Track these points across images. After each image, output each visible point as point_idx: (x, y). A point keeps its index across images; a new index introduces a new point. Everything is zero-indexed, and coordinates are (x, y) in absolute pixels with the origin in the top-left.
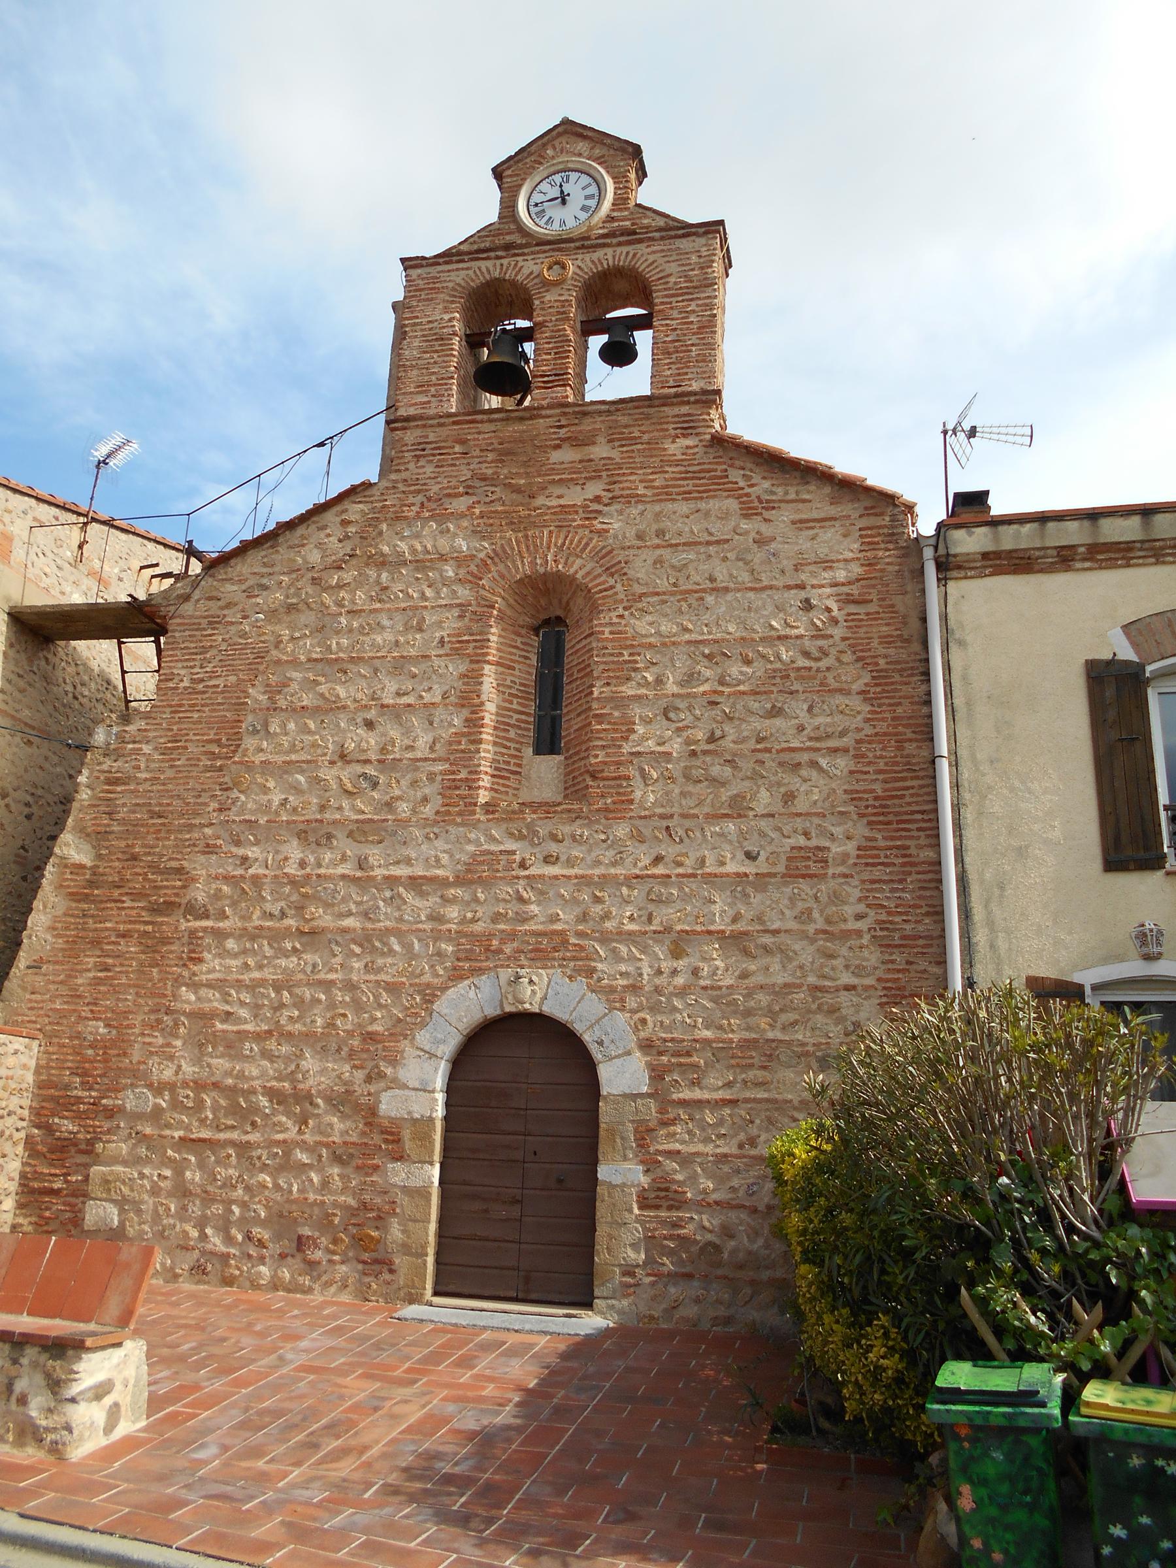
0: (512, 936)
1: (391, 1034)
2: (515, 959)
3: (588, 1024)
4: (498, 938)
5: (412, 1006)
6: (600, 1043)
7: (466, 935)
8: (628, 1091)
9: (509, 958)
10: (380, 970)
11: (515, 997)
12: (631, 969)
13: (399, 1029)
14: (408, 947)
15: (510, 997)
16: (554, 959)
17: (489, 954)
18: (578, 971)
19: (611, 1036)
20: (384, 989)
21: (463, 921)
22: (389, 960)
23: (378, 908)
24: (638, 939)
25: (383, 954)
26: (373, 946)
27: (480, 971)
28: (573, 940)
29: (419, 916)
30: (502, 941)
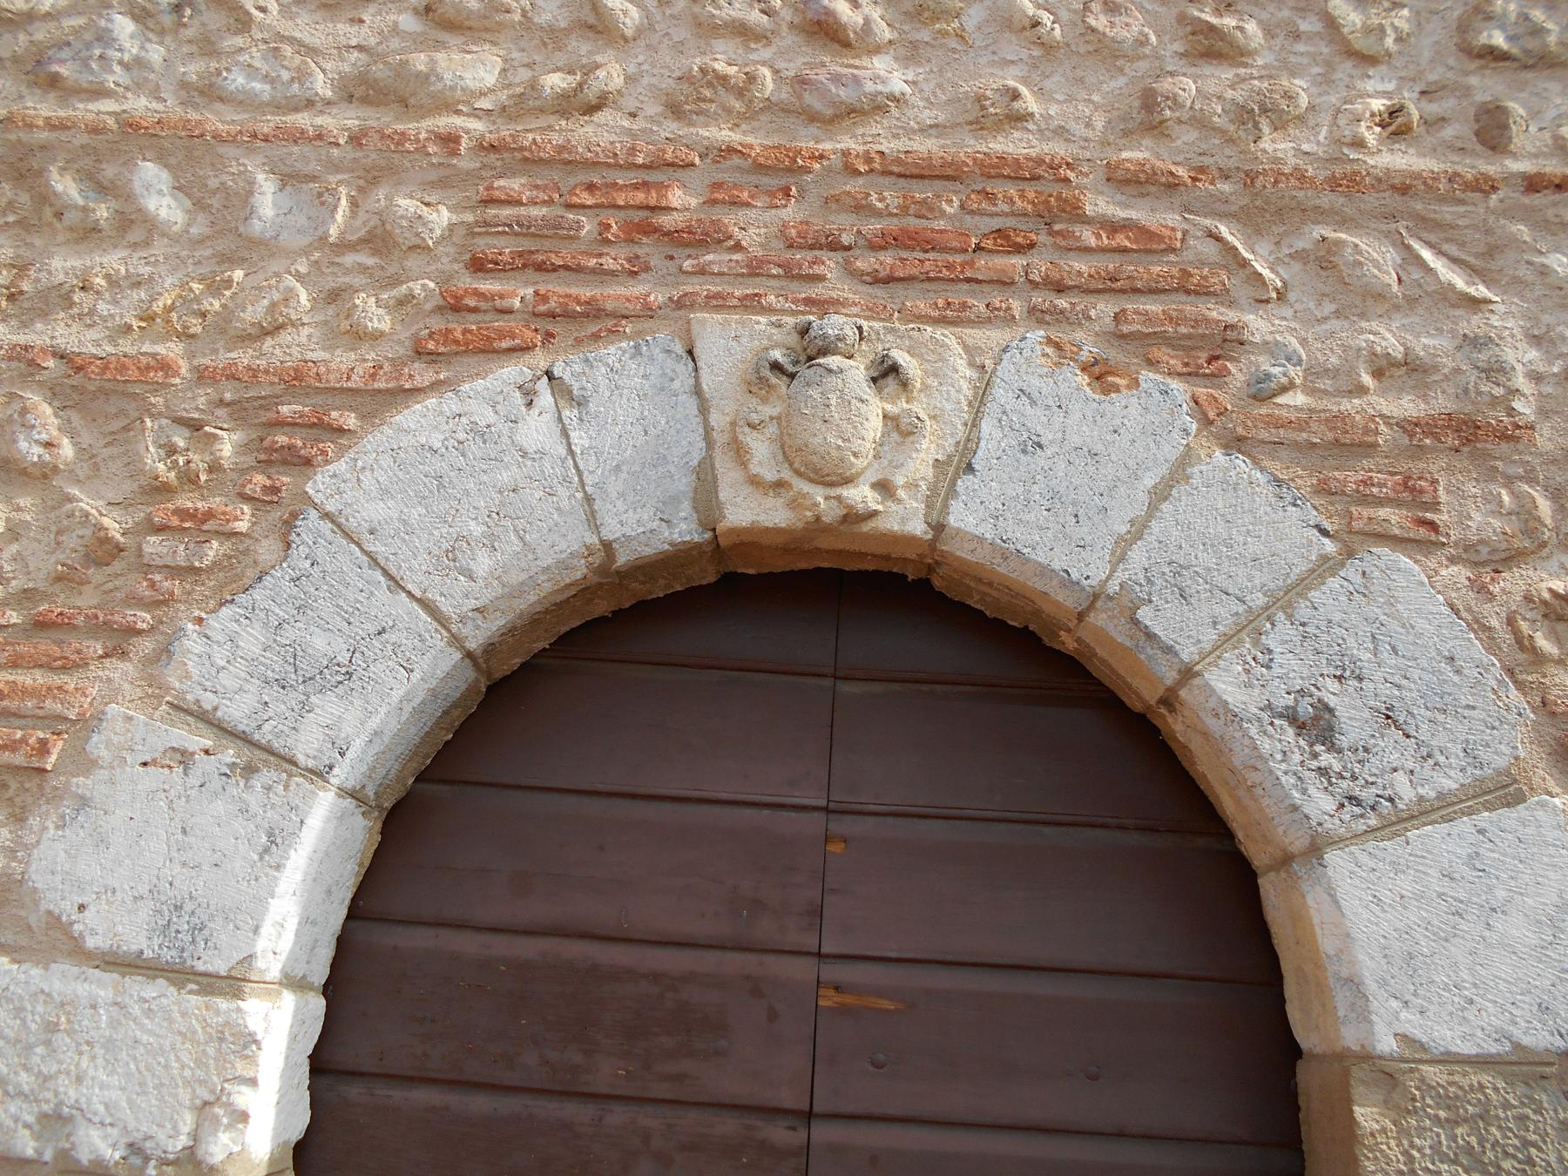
0: (781, 173)
1: (41, 625)
2: (791, 273)
3: (1227, 611)
4: (701, 177)
5: (189, 479)
6: (1317, 726)
7: (530, 161)
8: (1540, 1038)
9: (755, 269)
10: (57, 299)
11: (788, 451)
12: (1430, 344)
13: (87, 600)
14: (222, 210)
15: (760, 448)
16: (1004, 283)
17: (648, 249)
18: (1143, 344)
19: (1379, 689)
20: (54, 392)
21: (523, 104)
22: (115, 260)
23: (105, 38)
24: (1447, 212)
25: (88, 234)
26: (44, 198)
27: (596, 322)
28: (1099, 204)
29: (302, 75)
30: (720, 196)
